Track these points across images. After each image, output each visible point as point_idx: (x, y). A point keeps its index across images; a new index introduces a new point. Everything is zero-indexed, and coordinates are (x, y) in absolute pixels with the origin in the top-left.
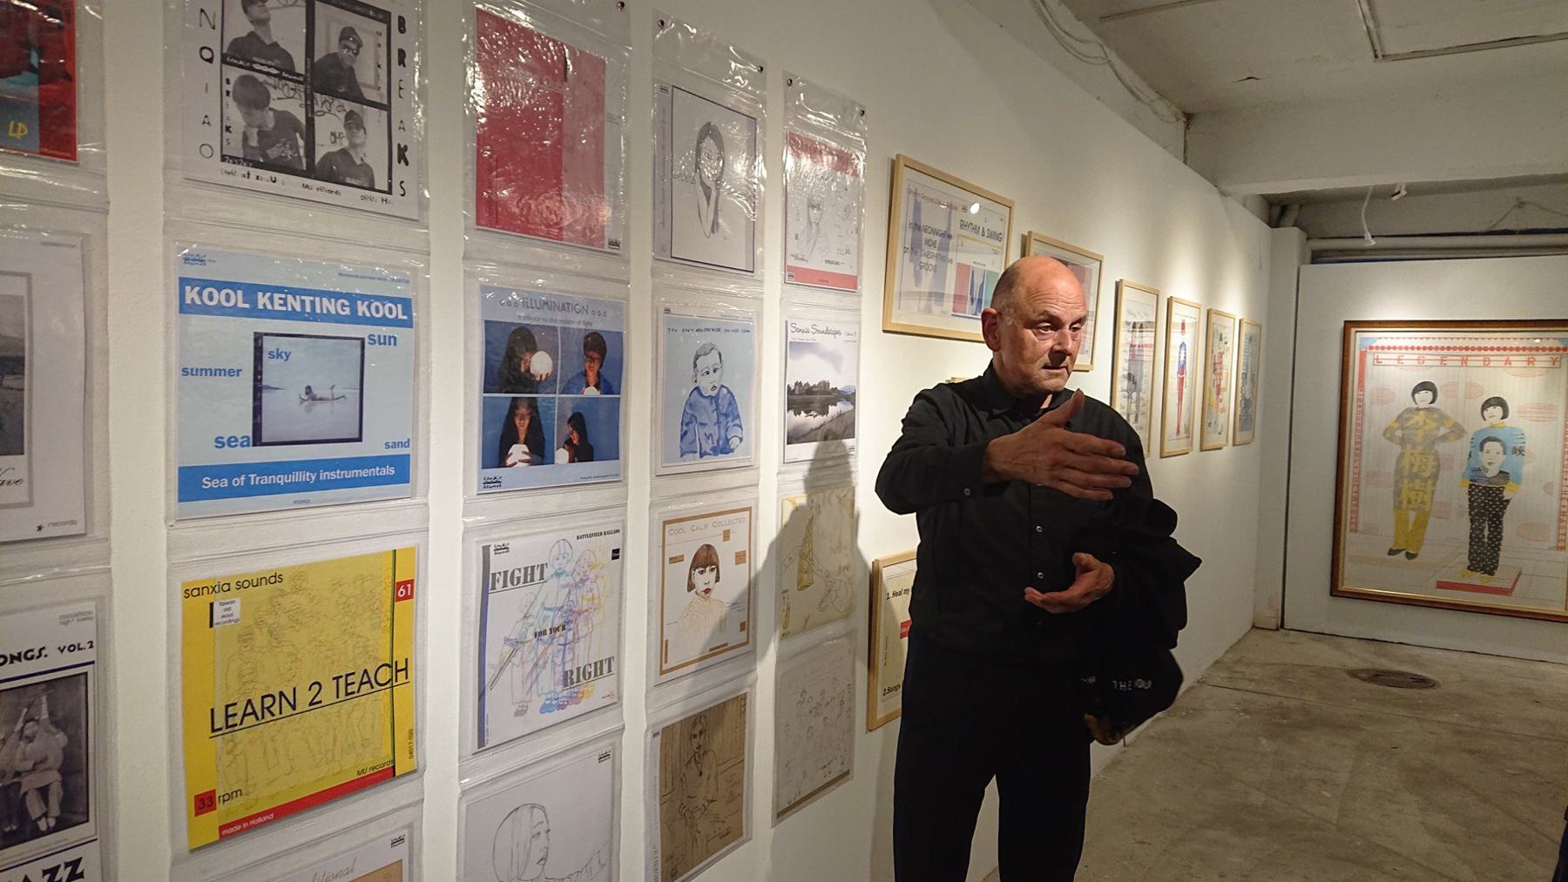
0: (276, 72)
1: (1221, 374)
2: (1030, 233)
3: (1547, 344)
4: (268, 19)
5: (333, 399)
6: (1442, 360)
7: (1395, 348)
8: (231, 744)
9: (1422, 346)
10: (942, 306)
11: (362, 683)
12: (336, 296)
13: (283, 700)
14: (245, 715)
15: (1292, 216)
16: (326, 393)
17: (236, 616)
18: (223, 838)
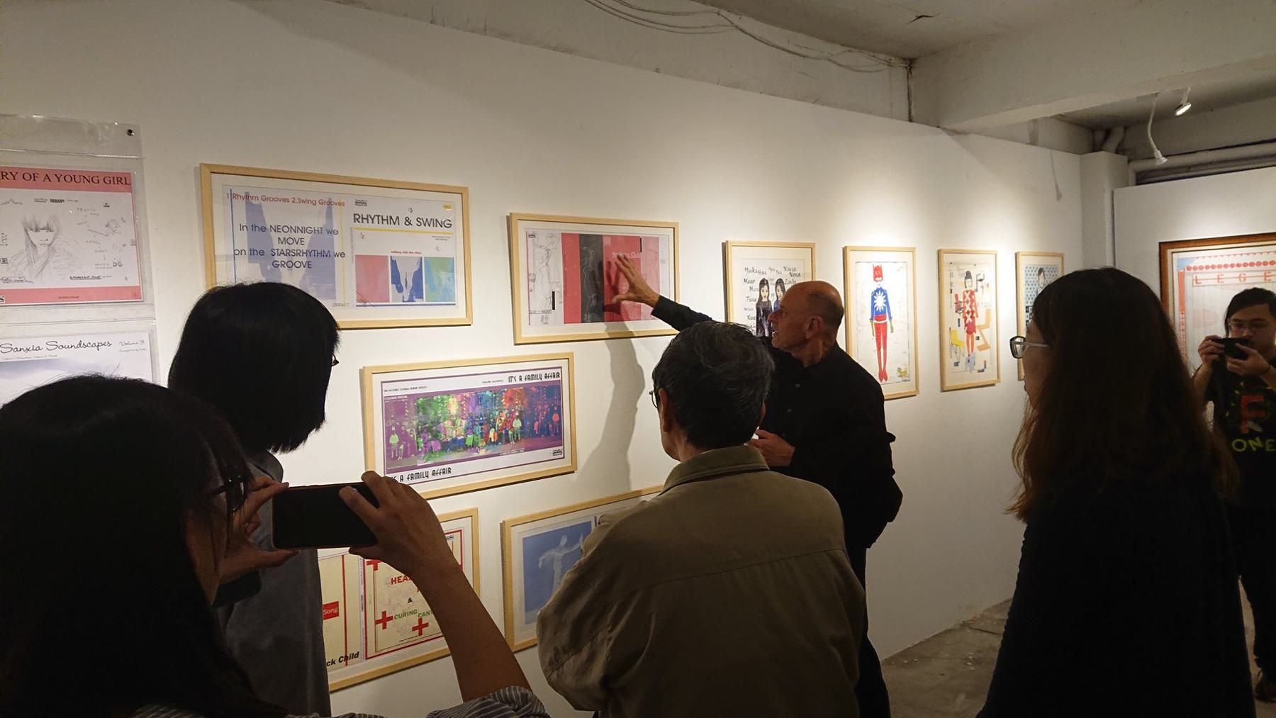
2: (511, 214)
6: (1266, 276)
7: (1213, 267)
9: (1242, 262)
10: (335, 298)
15: (1113, 142)
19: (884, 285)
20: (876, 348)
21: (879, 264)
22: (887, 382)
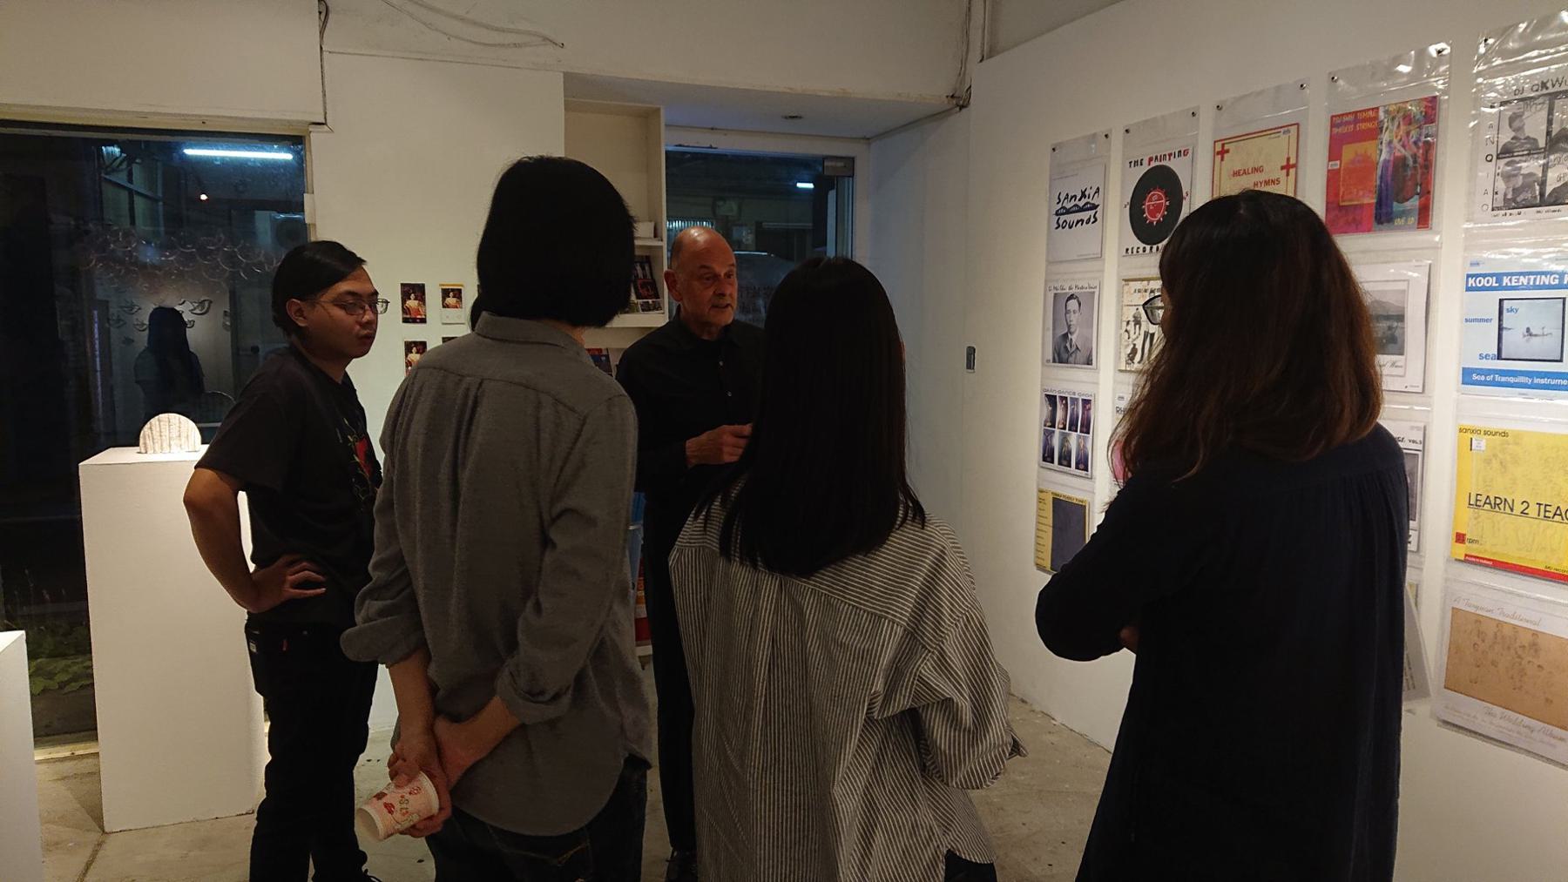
0: (1526, 152)
4: (1524, 125)
5: (1543, 335)
8: (1476, 515)
11: (1555, 514)
12: (1552, 273)
13: (1507, 505)
14: (1485, 503)
16: (1540, 332)
17: (1483, 448)
18: (1465, 561)
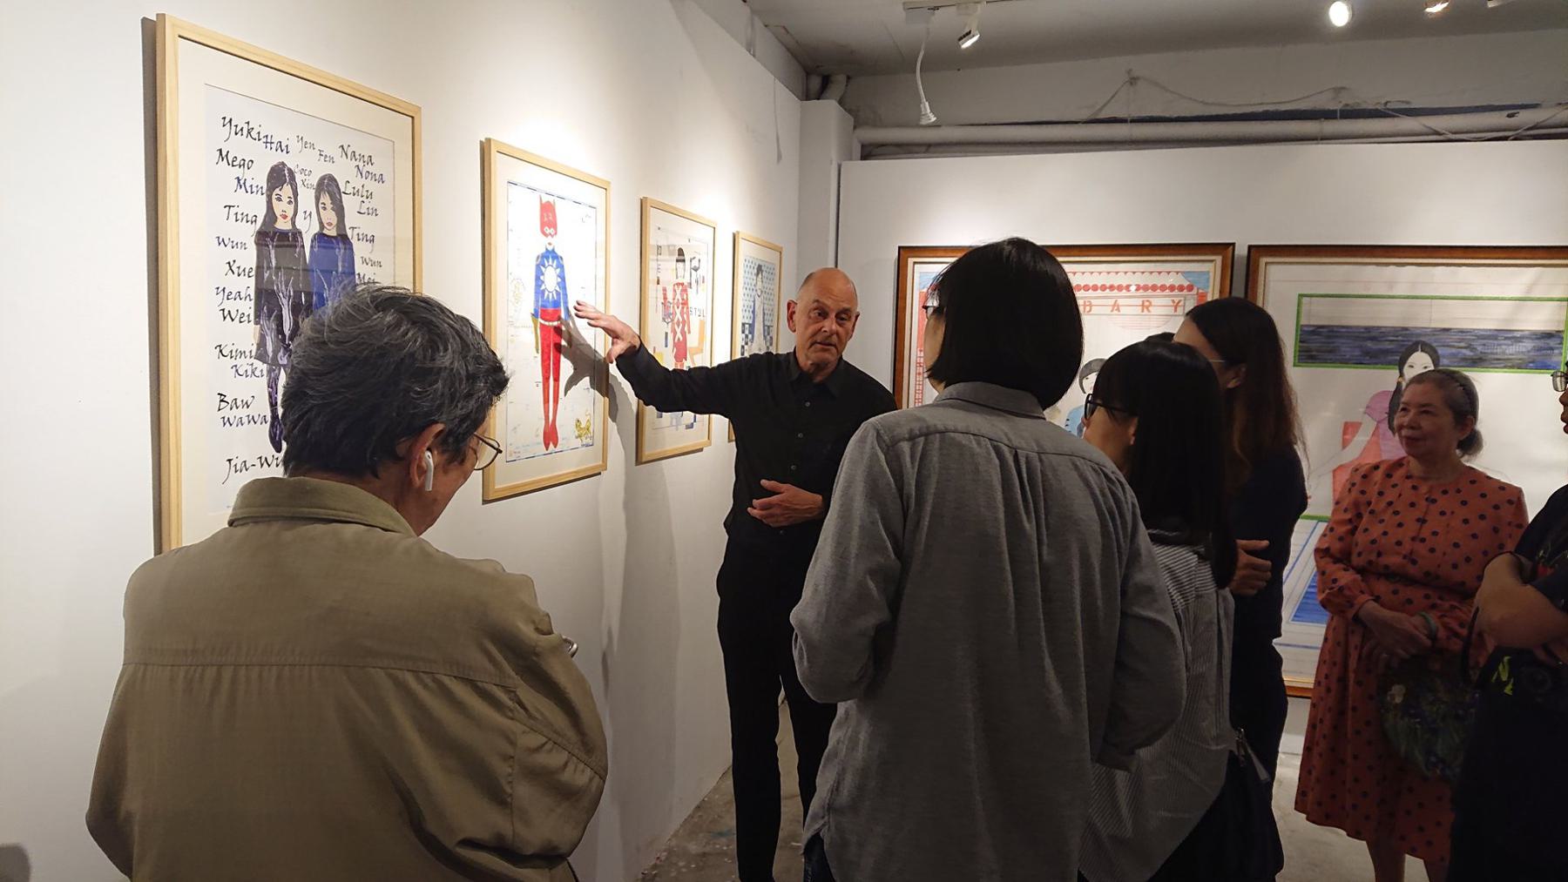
1: (685, 322)
3: (1170, 280)
19: (560, 245)
20: (541, 379)
21: (551, 199)
22: (558, 449)
